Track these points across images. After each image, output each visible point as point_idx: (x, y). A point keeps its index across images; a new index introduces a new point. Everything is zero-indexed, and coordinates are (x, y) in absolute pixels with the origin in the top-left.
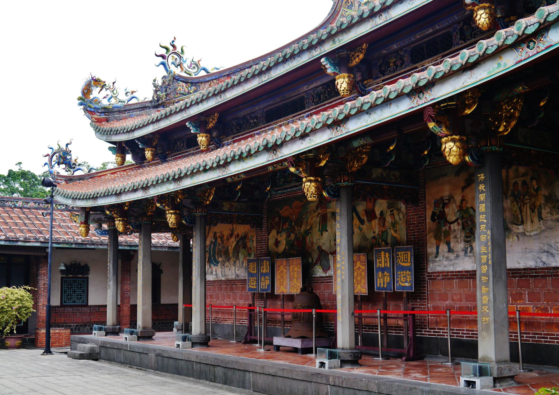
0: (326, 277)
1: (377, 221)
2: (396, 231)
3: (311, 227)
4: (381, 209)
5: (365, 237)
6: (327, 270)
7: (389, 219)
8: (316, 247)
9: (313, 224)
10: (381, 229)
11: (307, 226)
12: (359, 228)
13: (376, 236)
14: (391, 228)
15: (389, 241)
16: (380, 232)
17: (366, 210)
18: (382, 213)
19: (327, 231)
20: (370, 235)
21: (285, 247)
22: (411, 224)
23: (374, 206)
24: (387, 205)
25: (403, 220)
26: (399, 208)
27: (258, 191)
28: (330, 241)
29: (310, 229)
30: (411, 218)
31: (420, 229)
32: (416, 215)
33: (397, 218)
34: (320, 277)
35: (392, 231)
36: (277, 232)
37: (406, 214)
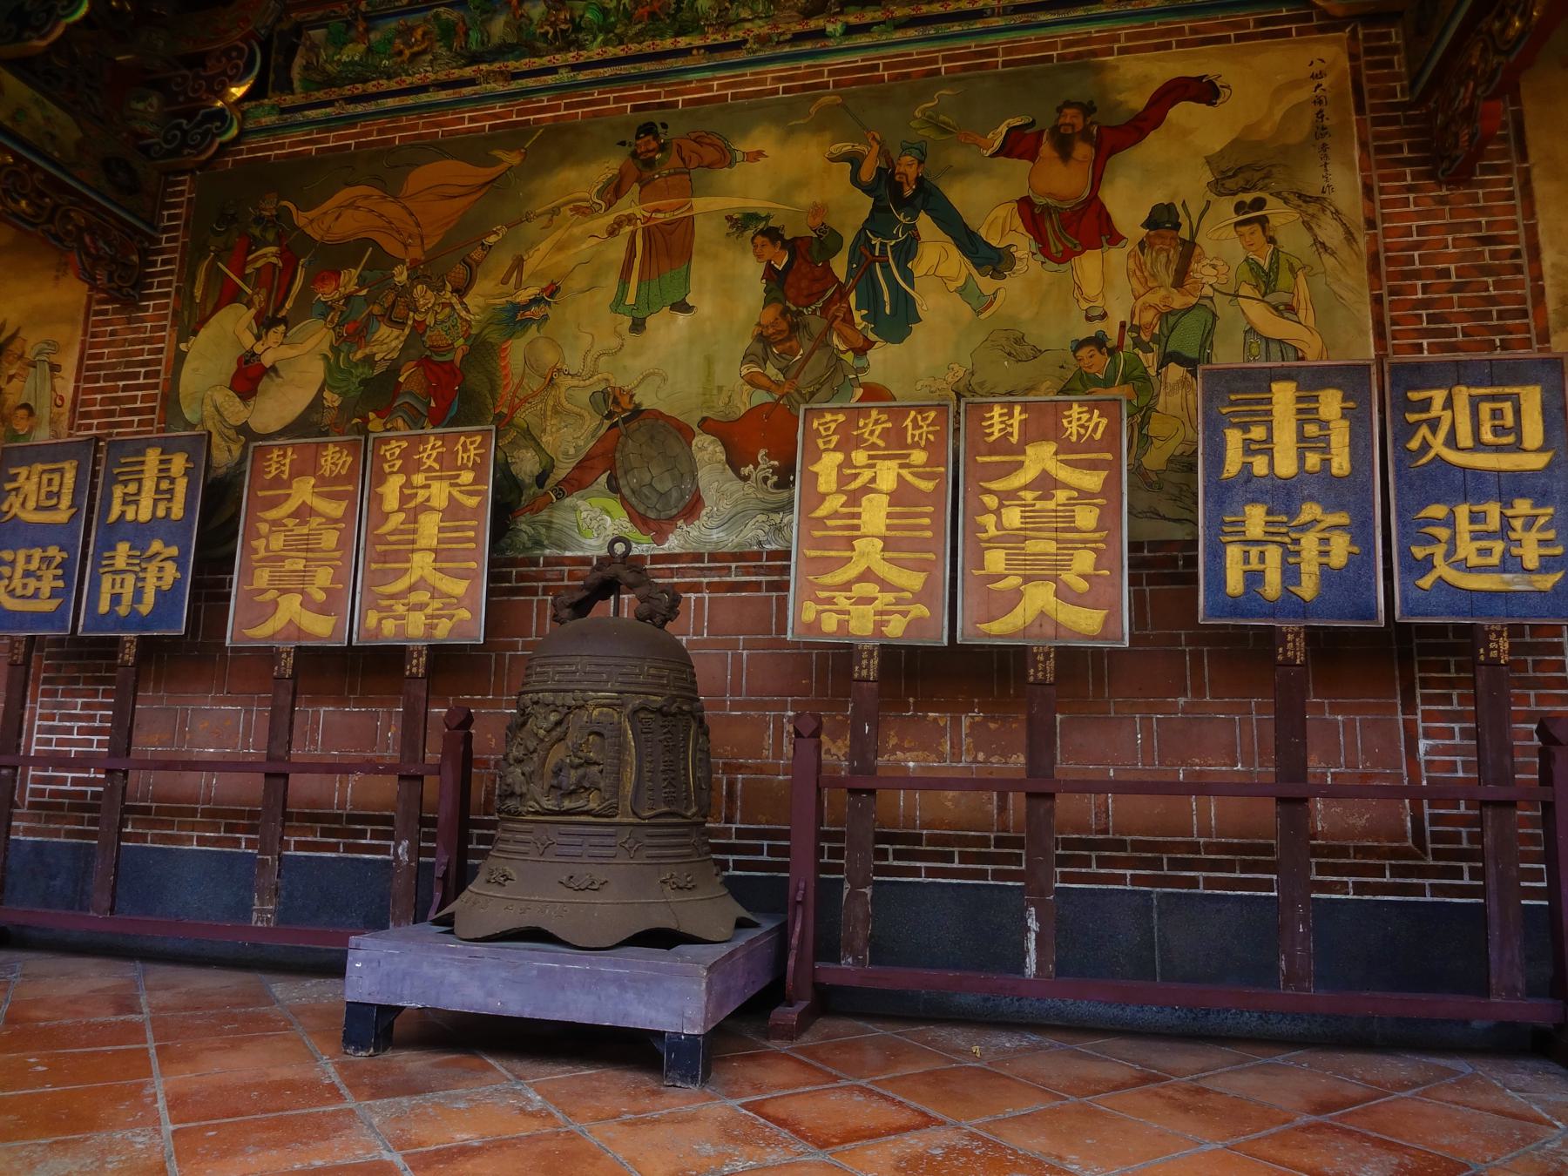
2: (1287, 310)
3: (553, 290)
4: (1160, 197)
5: (1020, 340)
6: (672, 520)
8: (584, 397)
9: (567, 276)
10: (1154, 298)
11: (518, 286)
13: (1113, 335)
14: (1246, 290)
16: (1149, 316)
18: (1162, 219)
19: (682, 307)
21: (319, 397)
22: (1417, 275)
24: (1208, 176)
25: (1345, 252)
26: (1314, 191)
27: (155, 101)
28: (709, 361)
29: (536, 301)
30: (1417, 246)
31: (1492, 301)
32: (1453, 228)
35: (1258, 313)
36: (256, 318)
37: (1371, 224)
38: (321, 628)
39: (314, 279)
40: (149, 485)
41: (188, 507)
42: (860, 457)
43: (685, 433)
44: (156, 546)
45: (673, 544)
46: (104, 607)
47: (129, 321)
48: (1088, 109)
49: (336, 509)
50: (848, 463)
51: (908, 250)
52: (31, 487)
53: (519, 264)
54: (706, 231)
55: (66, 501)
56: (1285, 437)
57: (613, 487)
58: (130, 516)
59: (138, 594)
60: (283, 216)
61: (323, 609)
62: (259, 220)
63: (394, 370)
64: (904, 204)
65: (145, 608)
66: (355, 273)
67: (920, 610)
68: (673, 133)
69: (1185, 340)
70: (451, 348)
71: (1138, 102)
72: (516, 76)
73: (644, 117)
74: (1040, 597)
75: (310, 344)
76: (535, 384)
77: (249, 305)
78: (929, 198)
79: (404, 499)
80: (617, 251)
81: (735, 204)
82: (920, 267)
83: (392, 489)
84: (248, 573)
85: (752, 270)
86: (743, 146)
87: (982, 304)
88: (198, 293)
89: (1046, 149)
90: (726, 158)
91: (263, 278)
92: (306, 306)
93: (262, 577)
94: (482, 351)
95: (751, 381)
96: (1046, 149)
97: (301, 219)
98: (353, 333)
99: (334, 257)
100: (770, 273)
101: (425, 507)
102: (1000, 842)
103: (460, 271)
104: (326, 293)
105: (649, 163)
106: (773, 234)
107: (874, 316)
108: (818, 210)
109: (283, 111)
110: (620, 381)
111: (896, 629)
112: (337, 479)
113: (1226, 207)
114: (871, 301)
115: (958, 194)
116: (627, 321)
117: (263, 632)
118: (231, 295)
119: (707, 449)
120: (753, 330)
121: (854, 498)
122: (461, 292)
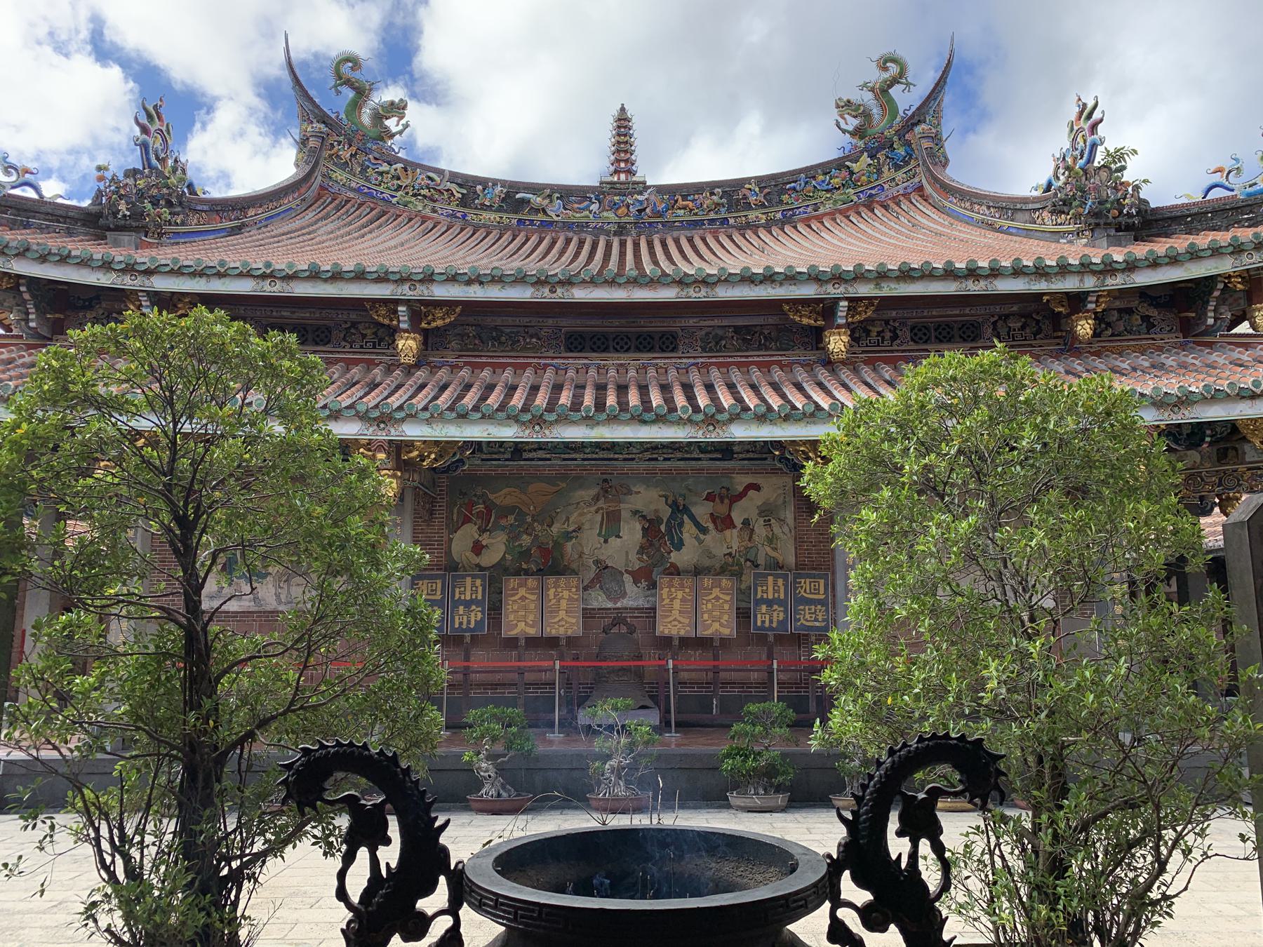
0: (614, 609)
1: (735, 532)
2: (775, 549)
7: (760, 531)
9: (583, 524)
12: (697, 538)
15: (761, 560)
17: (712, 514)
18: (746, 523)
19: (618, 536)
20: (720, 551)
23: (730, 510)
28: (627, 553)
29: (574, 531)
33: (777, 530)
34: (599, 609)
35: (768, 549)
38: (532, 632)
39: (498, 518)
40: (469, 588)
41: (483, 596)
42: (673, 590)
43: (620, 572)
44: (474, 607)
45: (619, 605)
46: (457, 626)
47: (428, 525)
48: (728, 489)
49: (533, 597)
50: (670, 591)
51: (681, 524)
52: (424, 587)
53: (568, 519)
54: (625, 514)
55: (439, 592)
56: (770, 589)
57: (601, 588)
58: (463, 598)
59: (469, 622)
60: (484, 495)
61: (532, 626)
62: (475, 495)
63: (529, 550)
64: (679, 511)
65: (472, 626)
66: (513, 517)
67: (688, 628)
68: (613, 483)
69: (751, 556)
70: (548, 543)
71: (740, 489)
72: (565, 460)
73: (605, 476)
74: (716, 626)
75: (499, 539)
76: (576, 556)
77: (475, 524)
78: (686, 510)
79: (555, 596)
80: (598, 518)
81: (634, 507)
82: (685, 530)
83: (552, 592)
84: (507, 616)
85: (638, 527)
86: (635, 489)
87: (701, 542)
88: (455, 519)
89: (717, 499)
90: (630, 492)
91: (479, 515)
92: (496, 527)
93: (512, 617)
94: (558, 545)
95: (639, 559)
96: (717, 499)
97: (491, 496)
98: (514, 537)
99: (506, 511)
100: (643, 528)
101: (562, 598)
102: (707, 683)
103: (548, 520)
104: (503, 522)
105: (607, 491)
106: (644, 517)
107: (672, 543)
108: (656, 511)
109: (483, 460)
110: (601, 557)
111: (682, 633)
112: (534, 589)
113: (761, 520)
114: (672, 539)
115: (693, 510)
116: (602, 540)
117: (513, 633)
118: (467, 520)
119: (628, 579)
120: (639, 545)
121: (672, 600)
122: (550, 526)
